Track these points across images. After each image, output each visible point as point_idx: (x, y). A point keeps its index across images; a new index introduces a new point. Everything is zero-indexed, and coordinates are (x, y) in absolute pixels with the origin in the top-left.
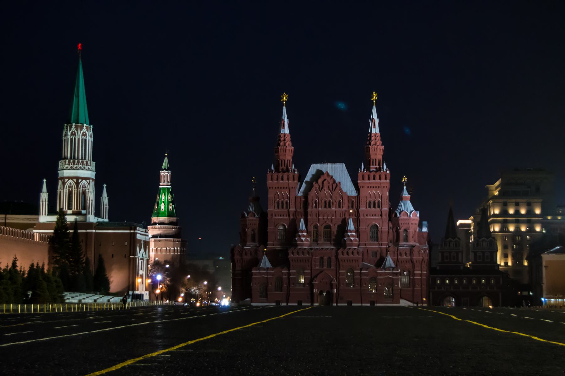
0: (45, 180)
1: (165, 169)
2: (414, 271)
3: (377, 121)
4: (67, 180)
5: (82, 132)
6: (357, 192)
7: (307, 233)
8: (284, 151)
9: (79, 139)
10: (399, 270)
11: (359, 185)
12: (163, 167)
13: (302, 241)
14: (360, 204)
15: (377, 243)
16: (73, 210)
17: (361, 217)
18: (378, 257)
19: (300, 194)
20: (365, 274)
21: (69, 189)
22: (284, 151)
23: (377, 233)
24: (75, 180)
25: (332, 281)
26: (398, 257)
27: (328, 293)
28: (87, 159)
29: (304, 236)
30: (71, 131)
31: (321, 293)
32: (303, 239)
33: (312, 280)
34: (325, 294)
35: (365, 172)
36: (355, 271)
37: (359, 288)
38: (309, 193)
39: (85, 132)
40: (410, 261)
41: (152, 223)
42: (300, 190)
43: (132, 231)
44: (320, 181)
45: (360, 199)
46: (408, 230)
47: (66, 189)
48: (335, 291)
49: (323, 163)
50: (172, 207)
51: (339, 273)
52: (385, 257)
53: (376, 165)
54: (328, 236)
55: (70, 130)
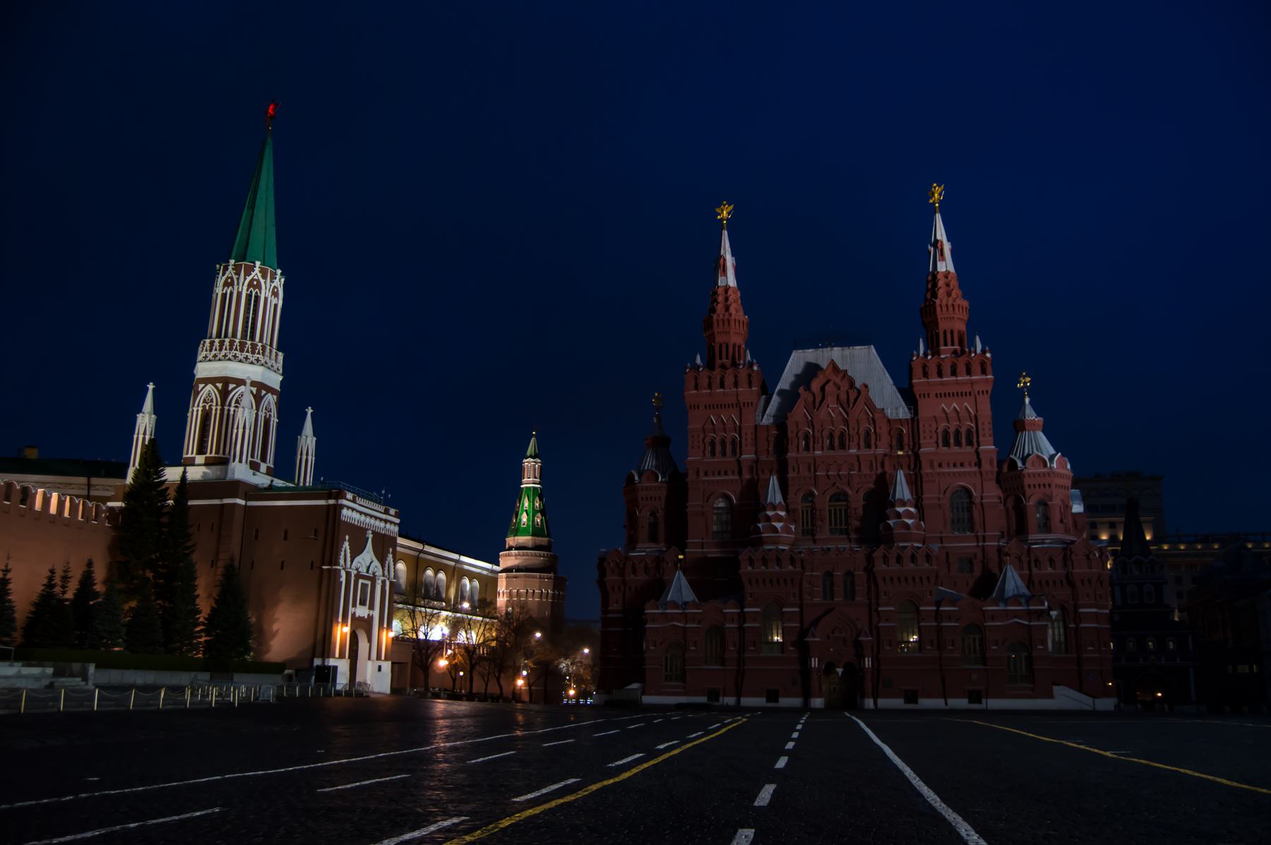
0: (151, 386)
1: (531, 457)
2: (1076, 607)
3: (947, 247)
4: (203, 385)
5: (249, 279)
6: (909, 409)
7: (787, 511)
8: (726, 323)
9: (239, 294)
10: (1046, 604)
11: (915, 389)
12: (528, 453)
13: (775, 530)
14: (921, 438)
15: (973, 534)
16: (208, 455)
17: (926, 470)
18: (978, 572)
19: (767, 420)
20: (950, 616)
21: (204, 407)
22: (726, 323)
23: (970, 510)
24: (220, 385)
25: (858, 636)
26: (1030, 569)
27: (848, 668)
28: (264, 342)
29: (779, 519)
30: (224, 278)
31: (829, 669)
32: (779, 525)
33: (803, 632)
34: (840, 670)
35: (929, 357)
36: (921, 608)
38: (789, 414)
39: (258, 281)
41: (507, 547)
42: (767, 412)
43: (332, 502)
44: (816, 385)
45: (921, 425)
46: (1049, 503)
47: (198, 406)
48: (868, 662)
49: (820, 348)
50: (541, 520)
51: (878, 612)
52: (996, 570)
53: (953, 345)
54: (841, 521)
55: (223, 275)
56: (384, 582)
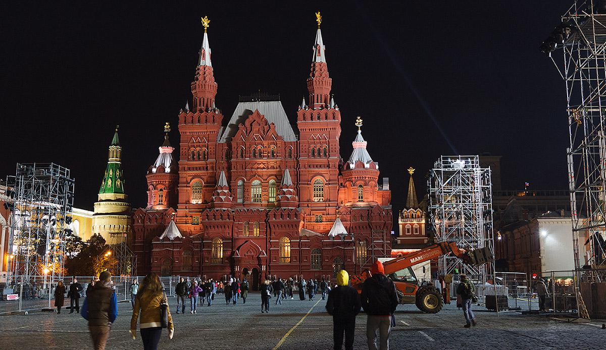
1: (114, 145)
3: (323, 48)
7: (230, 190)
8: (203, 87)
12: (113, 143)
19: (223, 141)
20: (306, 244)
22: (203, 87)
29: (224, 194)
32: (223, 197)
34: (250, 272)
35: (307, 109)
37: (298, 263)
40: (368, 227)
41: (99, 200)
42: (223, 136)
44: (247, 123)
45: (301, 145)
48: (264, 268)
50: (120, 183)
53: (321, 102)
56: (7, 229)
